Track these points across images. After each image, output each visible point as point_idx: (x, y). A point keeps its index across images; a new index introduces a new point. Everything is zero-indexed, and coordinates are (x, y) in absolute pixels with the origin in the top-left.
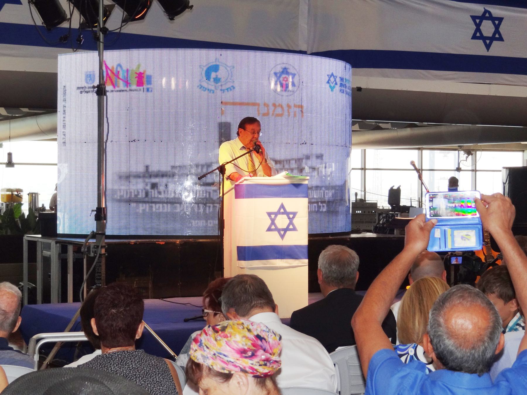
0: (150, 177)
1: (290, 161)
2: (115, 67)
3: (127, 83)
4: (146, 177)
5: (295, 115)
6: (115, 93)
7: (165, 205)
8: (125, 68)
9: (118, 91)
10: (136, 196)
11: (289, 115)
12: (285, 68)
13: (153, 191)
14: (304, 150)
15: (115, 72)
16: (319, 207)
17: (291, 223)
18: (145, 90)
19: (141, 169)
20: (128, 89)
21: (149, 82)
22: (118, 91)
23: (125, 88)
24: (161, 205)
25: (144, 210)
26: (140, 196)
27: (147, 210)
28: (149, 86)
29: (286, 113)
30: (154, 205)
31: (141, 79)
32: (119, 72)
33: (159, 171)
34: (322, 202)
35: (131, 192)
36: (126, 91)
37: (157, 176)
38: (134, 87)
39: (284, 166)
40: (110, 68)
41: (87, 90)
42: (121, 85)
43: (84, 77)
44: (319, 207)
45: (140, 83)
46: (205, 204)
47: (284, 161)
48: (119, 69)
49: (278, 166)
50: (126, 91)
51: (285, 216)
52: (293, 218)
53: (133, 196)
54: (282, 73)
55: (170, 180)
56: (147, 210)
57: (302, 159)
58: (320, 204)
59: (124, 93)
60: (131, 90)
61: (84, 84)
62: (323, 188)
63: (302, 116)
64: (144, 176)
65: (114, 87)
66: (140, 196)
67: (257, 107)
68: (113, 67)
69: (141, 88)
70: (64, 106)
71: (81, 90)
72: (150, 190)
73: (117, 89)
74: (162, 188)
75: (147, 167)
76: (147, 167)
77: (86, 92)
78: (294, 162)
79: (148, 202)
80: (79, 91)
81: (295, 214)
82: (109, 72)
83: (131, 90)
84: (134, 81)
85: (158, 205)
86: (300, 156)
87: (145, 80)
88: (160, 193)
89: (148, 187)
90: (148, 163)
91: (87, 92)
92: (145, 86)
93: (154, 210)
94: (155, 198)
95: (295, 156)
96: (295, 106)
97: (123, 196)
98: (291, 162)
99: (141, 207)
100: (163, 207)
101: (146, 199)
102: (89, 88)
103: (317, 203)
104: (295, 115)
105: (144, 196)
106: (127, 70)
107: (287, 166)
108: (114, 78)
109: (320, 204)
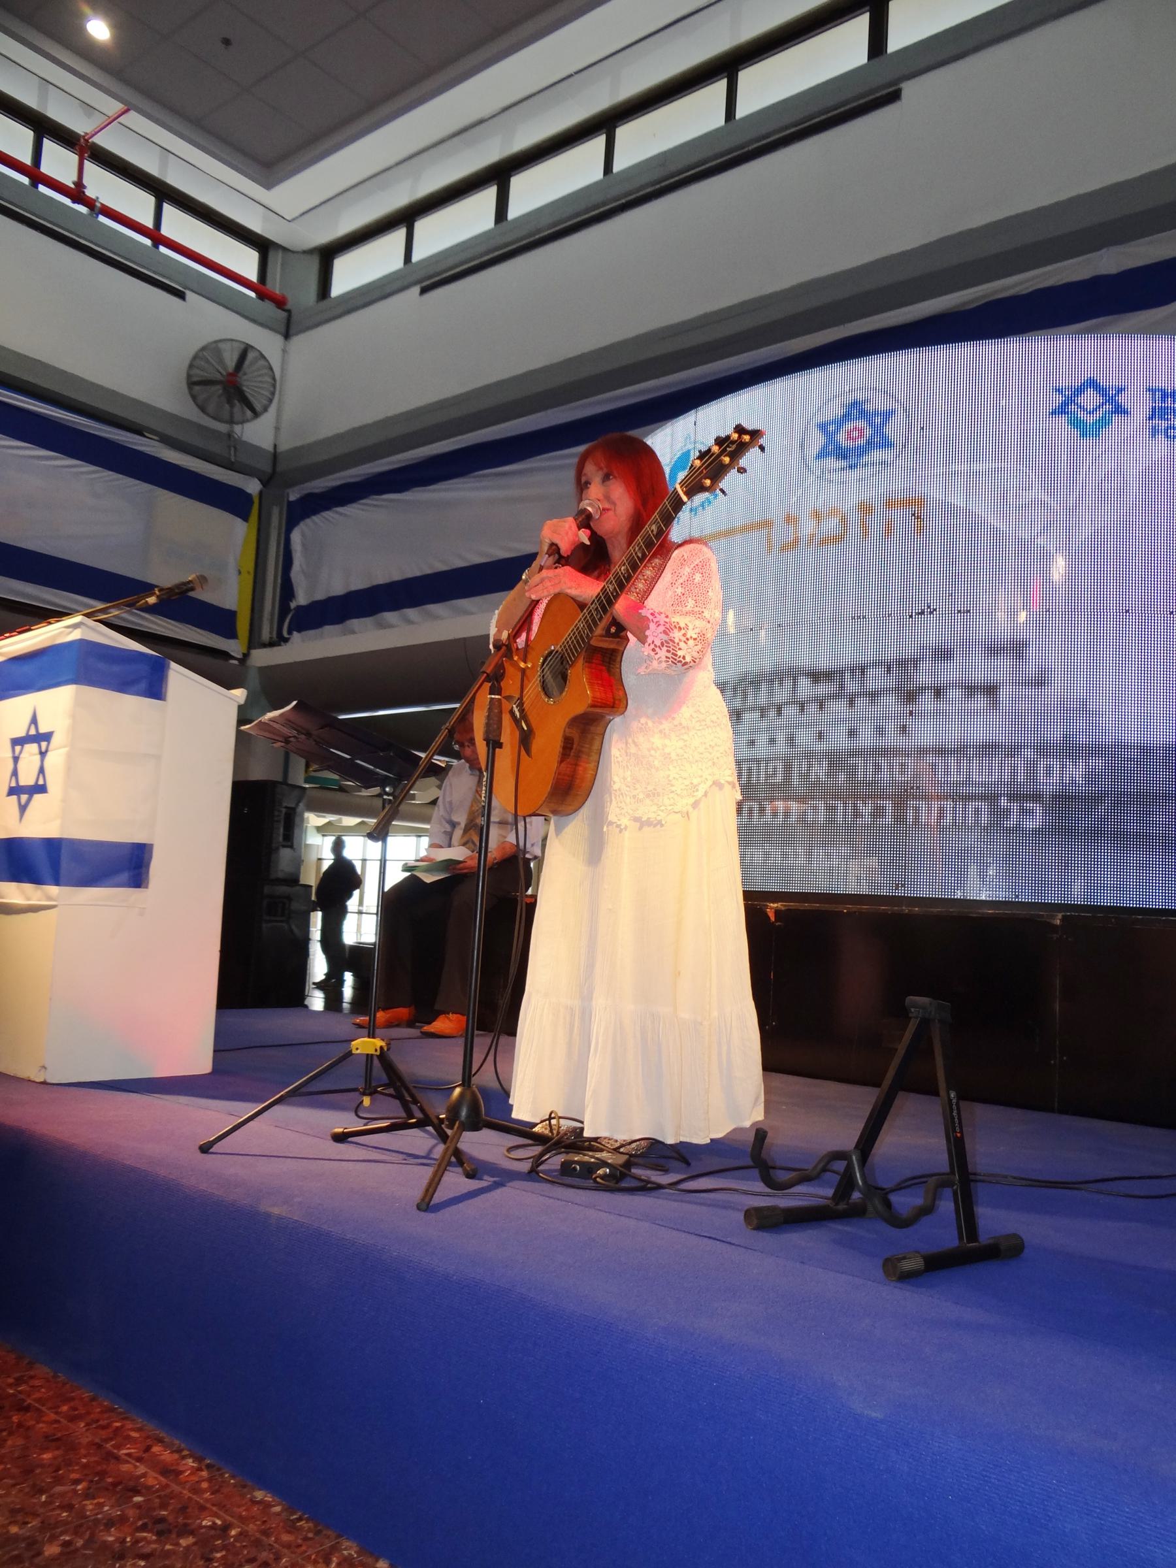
1: (863, 670)
5: (888, 530)
11: (866, 533)
12: (854, 404)
14: (931, 632)
16: (1000, 815)
17: (42, 770)
29: (854, 530)
34: (1012, 797)
39: (842, 687)
44: (1000, 815)
47: (842, 672)
49: (823, 689)
51: (35, 745)
52: (47, 751)
54: (846, 417)
57: (916, 662)
58: (1004, 802)
62: (1029, 753)
63: (920, 530)
67: (765, 531)
78: (881, 671)
81: (47, 737)
86: (909, 651)
95: (892, 654)
96: (889, 504)
98: (870, 672)
103: (991, 798)
104: (888, 530)
107: (851, 686)
109: (1004, 802)
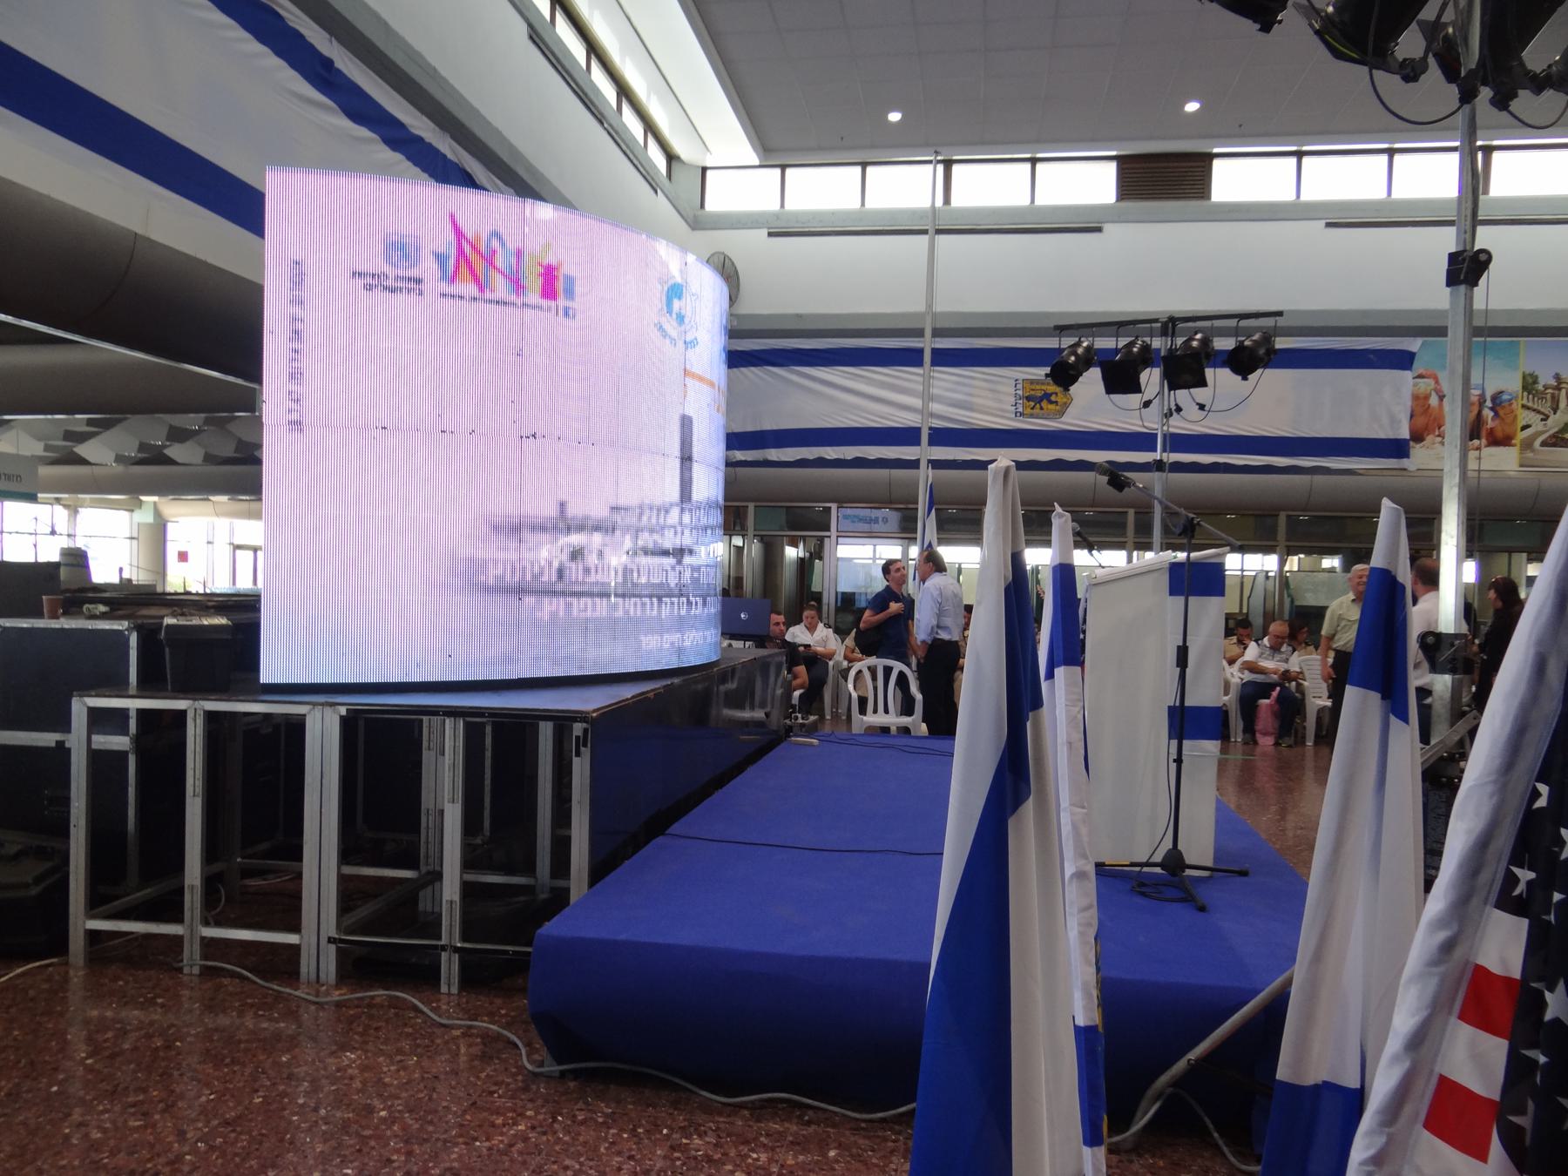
0: (569, 530)
2: (484, 237)
3: (518, 285)
4: (561, 531)
6: (481, 305)
7: (598, 600)
8: (512, 246)
9: (491, 301)
10: (535, 577)
13: (573, 565)
15: (483, 249)
18: (561, 312)
19: (549, 510)
20: (519, 302)
21: (570, 294)
22: (491, 301)
23: (513, 298)
24: (589, 601)
25: (554, 615)
26: (545, 578)
27: (561, 613)
28: (569, 304)
30: (574, 601)
31: (550, 283)
32: (494, 252)
33: (587, 518)
35: (524, 568)
36: (514, 304)
37: (581, 528)
38: (534, 297)
40: (470, 234)
41: (390, 283)
42: (501, 287)
43: (380, 248)
45: (549, 291)
46: (660, 598)
48: (495, 244)
50: (514, 304)
53: (528, 577)
55: (608, 539)
56: (561, 613)
59: (509, 310)
60: (524, 305)
61: (377, 264)
64: (555, 529)
65: (481, 289)
66: (545, 578)
68: (478, 238)
69: (552, 304)
70: (294, 319)
71: (369, 280)
72: (567, 564)
73: (488, 295)
74: (592, 560)
75: (562, 505)
76: (562, 505)
77: (385, 288)
79: (563, 594)
80: (360, 282)
82: (467, 249)
83: (524, 305)
84: (534, 283)
85: (583, 600)
87: (560, 285)
88: (587, 571)
89: (565, 557)
90: (564, 498)
91: (393, 290)
92: (562, 302)
93: (575, 612)
94: (577, 582)
97: (504, 577)
99: (550, 606)
100: (594, 605)
101: (559, 587)
102: (397, 278)
105: (554, 578)
106: (519, 254)
108: (479, 266)
